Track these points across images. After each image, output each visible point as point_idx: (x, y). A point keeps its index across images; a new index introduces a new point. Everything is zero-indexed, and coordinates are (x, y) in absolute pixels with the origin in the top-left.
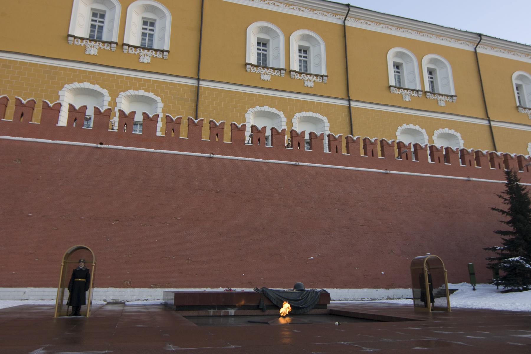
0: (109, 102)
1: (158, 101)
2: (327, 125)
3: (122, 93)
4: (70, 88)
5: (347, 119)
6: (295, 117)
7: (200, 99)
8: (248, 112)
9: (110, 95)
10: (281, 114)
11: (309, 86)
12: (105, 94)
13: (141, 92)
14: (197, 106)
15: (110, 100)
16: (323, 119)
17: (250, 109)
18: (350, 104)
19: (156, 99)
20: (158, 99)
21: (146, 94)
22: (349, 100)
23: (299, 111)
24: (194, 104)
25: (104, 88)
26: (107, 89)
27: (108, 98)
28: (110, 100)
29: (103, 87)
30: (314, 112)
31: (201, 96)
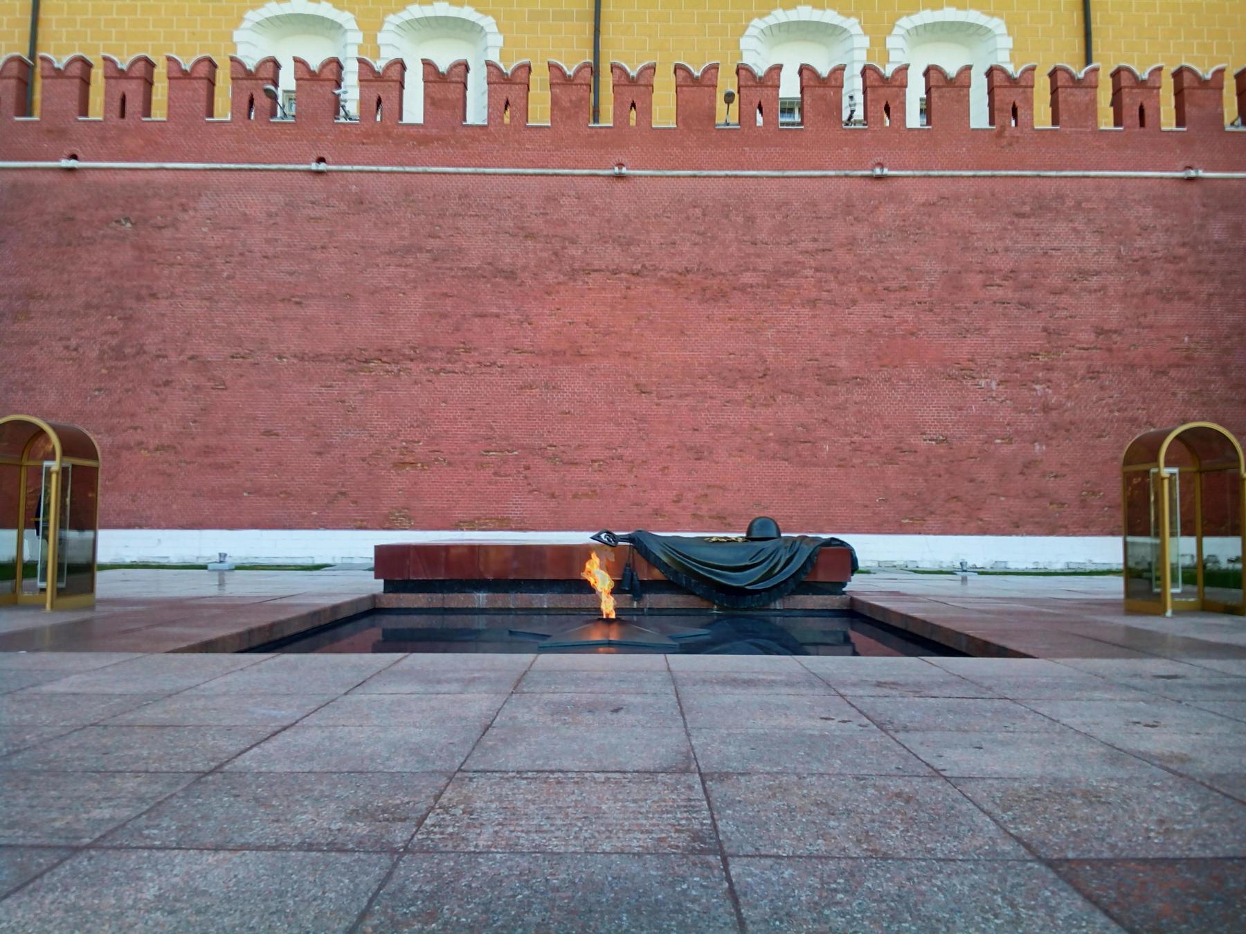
0: (360, 46)
1: (487, 29)
2: (1008, 42)
6: (896, 31)
10: (852, 25)
15: (360, 41)
17: (756, 22)
19: (482, 23)
20: (488, 23)
21: (454, 12)
23: (914, 9)
24: (589, 26)
27: (355, 37)
28: (360, 41)
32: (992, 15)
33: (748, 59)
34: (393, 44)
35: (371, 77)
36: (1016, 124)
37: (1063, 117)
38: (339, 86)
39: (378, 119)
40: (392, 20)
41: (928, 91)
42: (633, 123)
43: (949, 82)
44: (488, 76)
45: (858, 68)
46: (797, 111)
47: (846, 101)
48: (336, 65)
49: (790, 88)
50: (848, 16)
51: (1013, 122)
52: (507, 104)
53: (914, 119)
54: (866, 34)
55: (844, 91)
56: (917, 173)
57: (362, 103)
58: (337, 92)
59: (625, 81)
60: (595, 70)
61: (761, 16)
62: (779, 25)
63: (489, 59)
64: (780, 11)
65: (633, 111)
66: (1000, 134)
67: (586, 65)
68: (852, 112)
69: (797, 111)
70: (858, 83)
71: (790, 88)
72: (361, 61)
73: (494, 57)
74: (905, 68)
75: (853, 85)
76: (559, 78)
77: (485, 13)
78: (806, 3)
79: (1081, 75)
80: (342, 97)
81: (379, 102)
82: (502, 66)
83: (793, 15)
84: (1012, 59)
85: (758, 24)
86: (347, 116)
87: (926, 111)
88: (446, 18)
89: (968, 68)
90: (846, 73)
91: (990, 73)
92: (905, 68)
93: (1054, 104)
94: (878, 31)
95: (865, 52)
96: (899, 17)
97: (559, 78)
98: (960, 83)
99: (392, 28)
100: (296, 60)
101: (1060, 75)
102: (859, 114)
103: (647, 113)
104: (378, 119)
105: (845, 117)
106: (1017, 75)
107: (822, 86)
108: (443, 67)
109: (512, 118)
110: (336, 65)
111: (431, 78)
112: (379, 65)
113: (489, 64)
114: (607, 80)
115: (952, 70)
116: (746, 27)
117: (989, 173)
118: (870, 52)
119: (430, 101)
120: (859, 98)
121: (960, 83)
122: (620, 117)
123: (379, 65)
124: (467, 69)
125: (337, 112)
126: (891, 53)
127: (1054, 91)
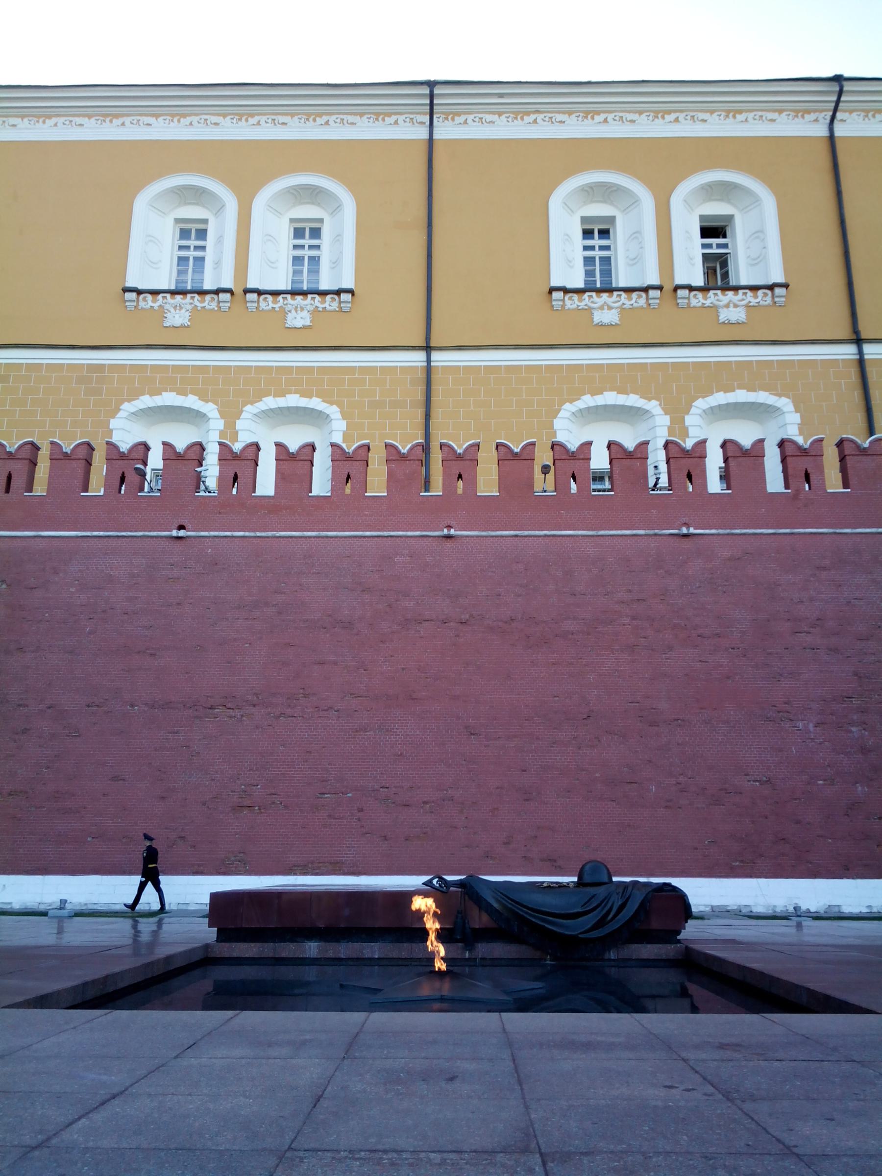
1: (332, 416)
2: (796, 418)
3: (248, 408)
4: (133, 410)
5: (857, 395)
7: (433, 399)
8: (562, 414)
9: (222, 415)
10: (653, 406)
11: (733, 319)
12: (210, 415)
13: (293, 400)
14: (428, 416)
15: (222, 428)
16: (778, 404)
17: (567, 406)
18: (861, 352)
19: (327, 411)
20: (333, 411)
21: (303, 402)
22: (858, 341)
23: (707, 392)
24: (420, 412)
25: (207, 401)
26: (216, 403)
27: (217, 424)
28: (222, 428)
29: (204, 398)
30: (751, 389)
31: (438, 389)
32: (780, 395)
33: (561, 437)
34: (248, 430)
35: (229, 457)
36: (810, 488)
37: (853, 480)
38: (201, 465)
39: (234, 491)
40: (250, 410)
41: (726, 460)
42: (460, 491)
43: (745, 453)
44: (332, 455)
45: (661, 443)
46: (607, 479)
47: (651, 471)
48: (200, 447)
49: (600, 460)
50: (649, 399)
51: (807, 486)
52: (348, 477)
53: (714, 485)
54: (666, 414)
55: (649, 461)
56: (721, 531)
57: (221, 479)
58: (198, 469)
59: (451, 456)
60: (426, 448)
61: (571, 401)
62: (589, 409)
63: (333, 441)
64: (589, 396)
65: (460, 482)
66: (796, 496)
67: (418, 445)
68: (658, 479)
69: (607, 479)
70: (662, 455)
71: (600, 460)
72: (221, 444)
73: (338, 439)
74: (704, 441)
75: (657, 457)
76: (393, 455)
77: (331, 403)
78: (611, 390)
79: (866, 445)
80: (202, 474)
81: (235, 478)
82: (344, 446)
83: (601, 400)
84: (801, 433)
85: (569, 408)
86: (207, 490)
87: (725, 476)
88: (297, 408)
89: (761, 441)
90: (650, 447)
91: (782, 444)
92: (704, 441)
93: (844, 470)
94: (677, 413)
95: (666, 429)
96: (697, 398)
97: (393, 455)
98: (757, 451)
99: (250, 416)
100: (165, 444)
101: (846, 445)
102: (664, 481)
103: (472, 484)
104: (234, 491)
105: (651, 483)
106: (807, 446)
107: (627, 459)
108: (293, 447)
109: (352, 489)
110: (200, 447)
111: (281, 458)
112: (237, 447)
113: (333, 445)
114: (437, 456)
115: (746, 442)
116: (559, 411)
117: (788, 531)
118: (671, 430)
119: (281, 477)
120: (663, 467)
121: (757, 451)
122: (448, 487)
123: (237, 447)
124: (314, 449)
125: (198, 487)
126: (690, 429)
127: (842, 459)
